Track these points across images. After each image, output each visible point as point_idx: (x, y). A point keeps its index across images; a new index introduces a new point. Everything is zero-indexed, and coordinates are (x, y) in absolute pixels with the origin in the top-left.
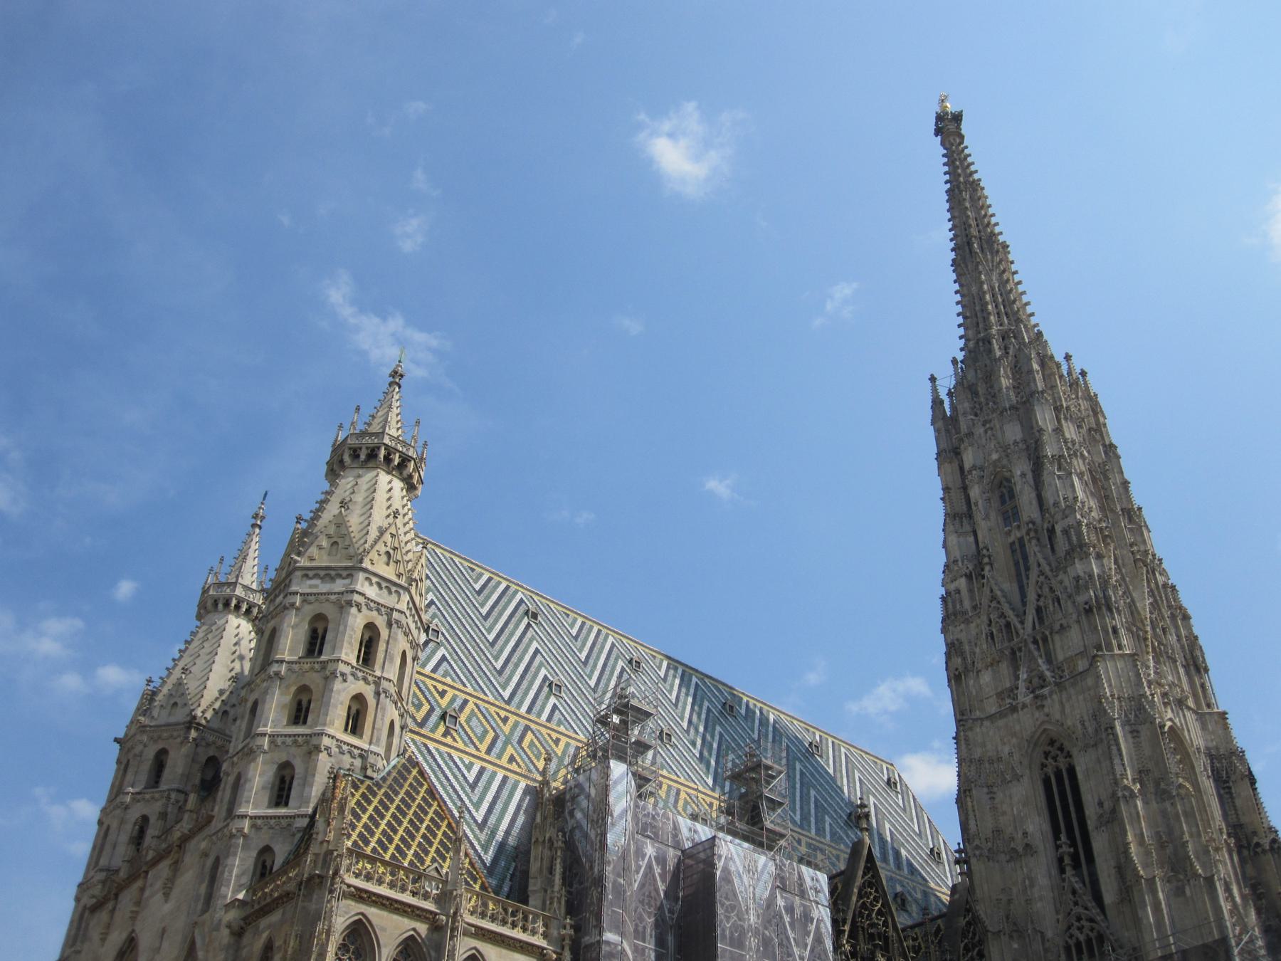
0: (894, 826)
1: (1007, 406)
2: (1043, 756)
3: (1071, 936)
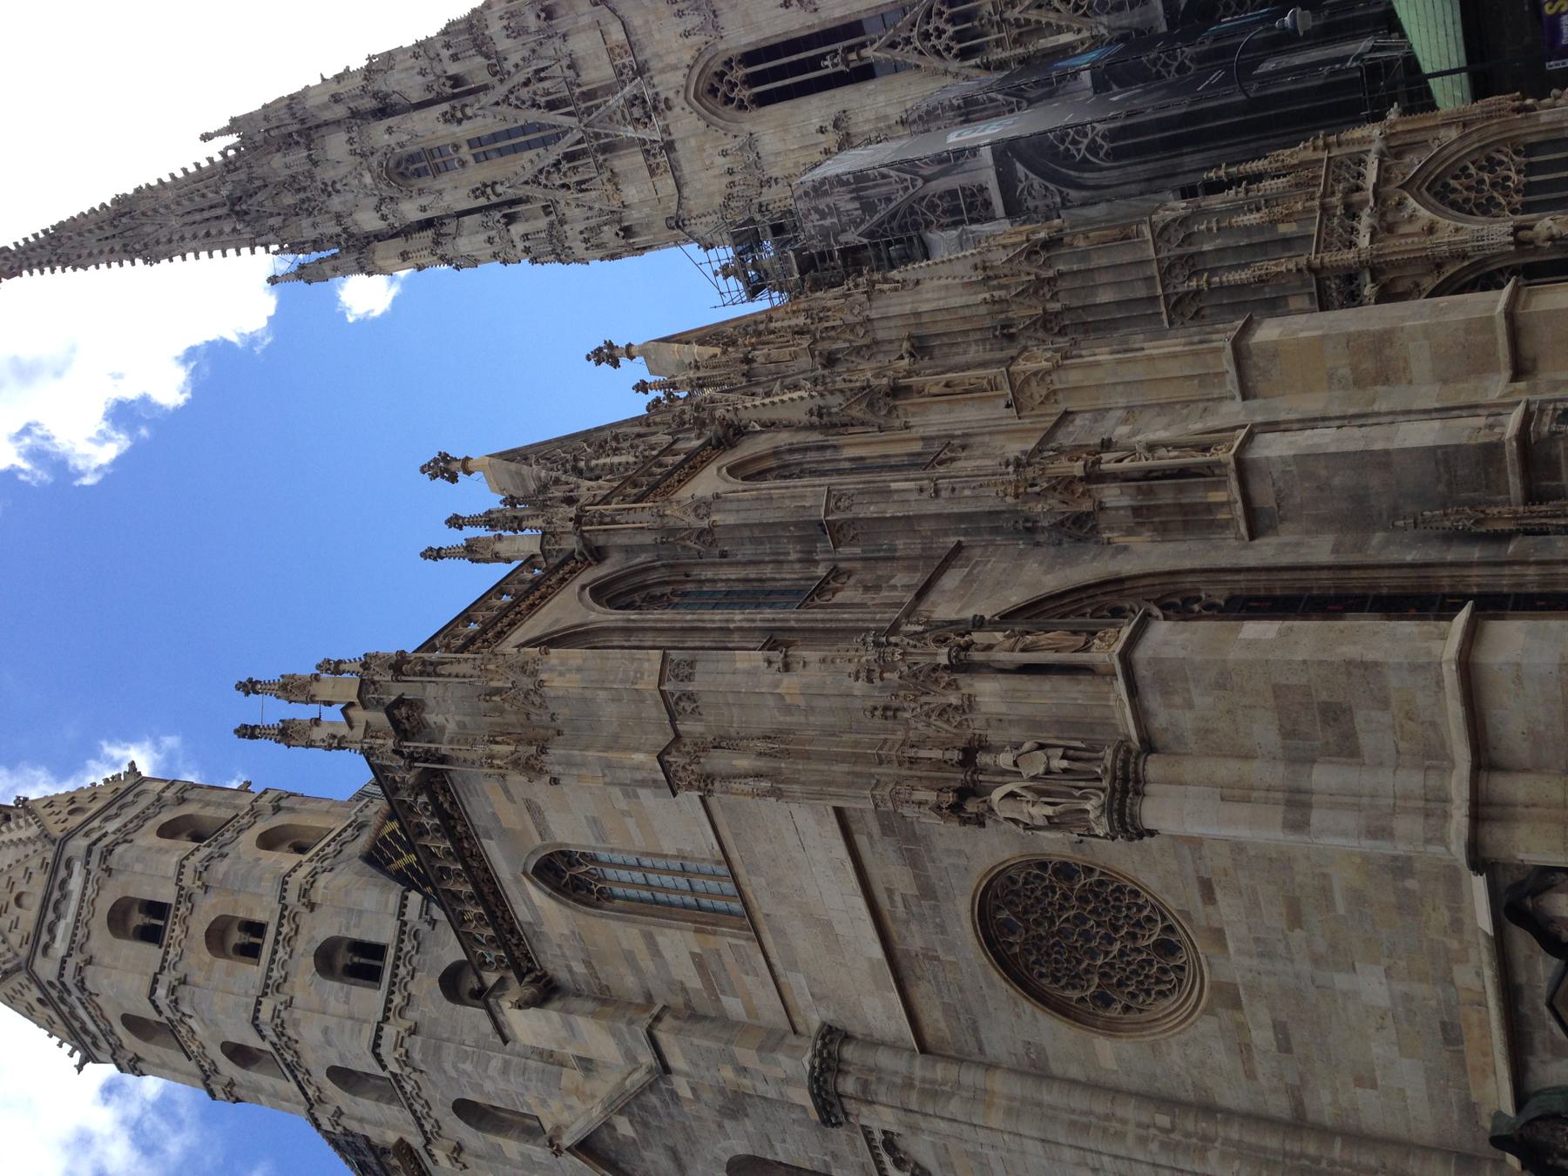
1: (306, 154)
2: (730, 106)
3: (948, 49)
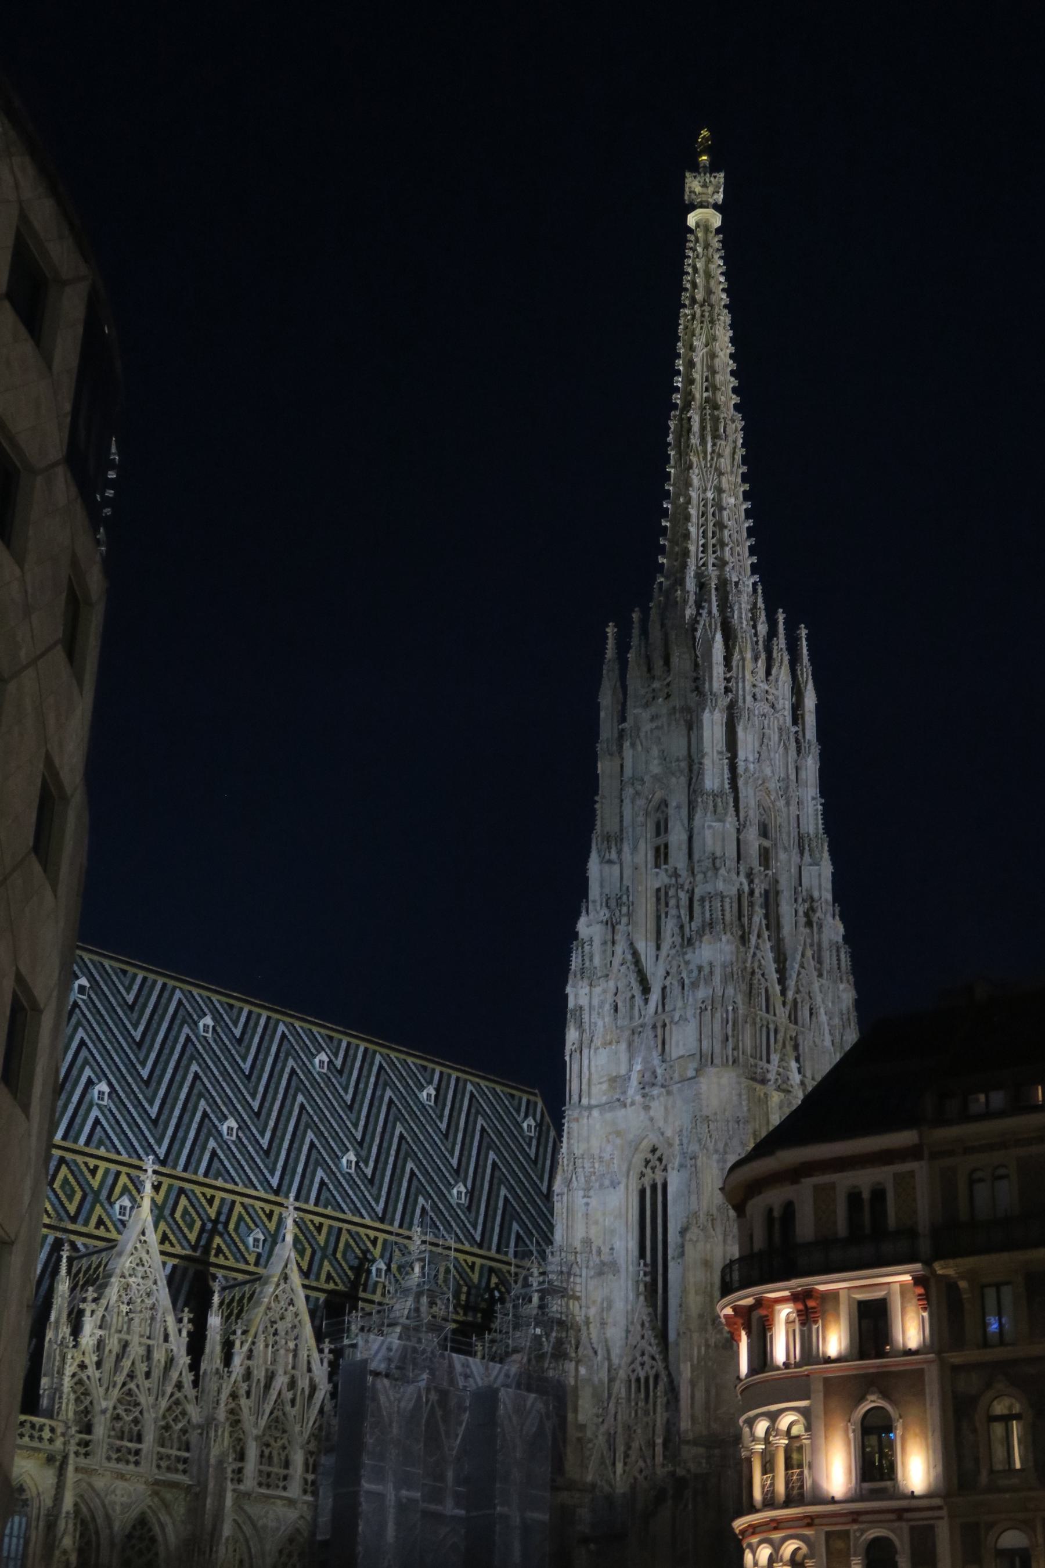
0: (511, 1189)
